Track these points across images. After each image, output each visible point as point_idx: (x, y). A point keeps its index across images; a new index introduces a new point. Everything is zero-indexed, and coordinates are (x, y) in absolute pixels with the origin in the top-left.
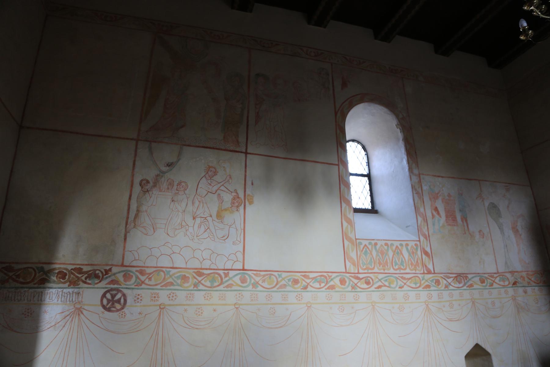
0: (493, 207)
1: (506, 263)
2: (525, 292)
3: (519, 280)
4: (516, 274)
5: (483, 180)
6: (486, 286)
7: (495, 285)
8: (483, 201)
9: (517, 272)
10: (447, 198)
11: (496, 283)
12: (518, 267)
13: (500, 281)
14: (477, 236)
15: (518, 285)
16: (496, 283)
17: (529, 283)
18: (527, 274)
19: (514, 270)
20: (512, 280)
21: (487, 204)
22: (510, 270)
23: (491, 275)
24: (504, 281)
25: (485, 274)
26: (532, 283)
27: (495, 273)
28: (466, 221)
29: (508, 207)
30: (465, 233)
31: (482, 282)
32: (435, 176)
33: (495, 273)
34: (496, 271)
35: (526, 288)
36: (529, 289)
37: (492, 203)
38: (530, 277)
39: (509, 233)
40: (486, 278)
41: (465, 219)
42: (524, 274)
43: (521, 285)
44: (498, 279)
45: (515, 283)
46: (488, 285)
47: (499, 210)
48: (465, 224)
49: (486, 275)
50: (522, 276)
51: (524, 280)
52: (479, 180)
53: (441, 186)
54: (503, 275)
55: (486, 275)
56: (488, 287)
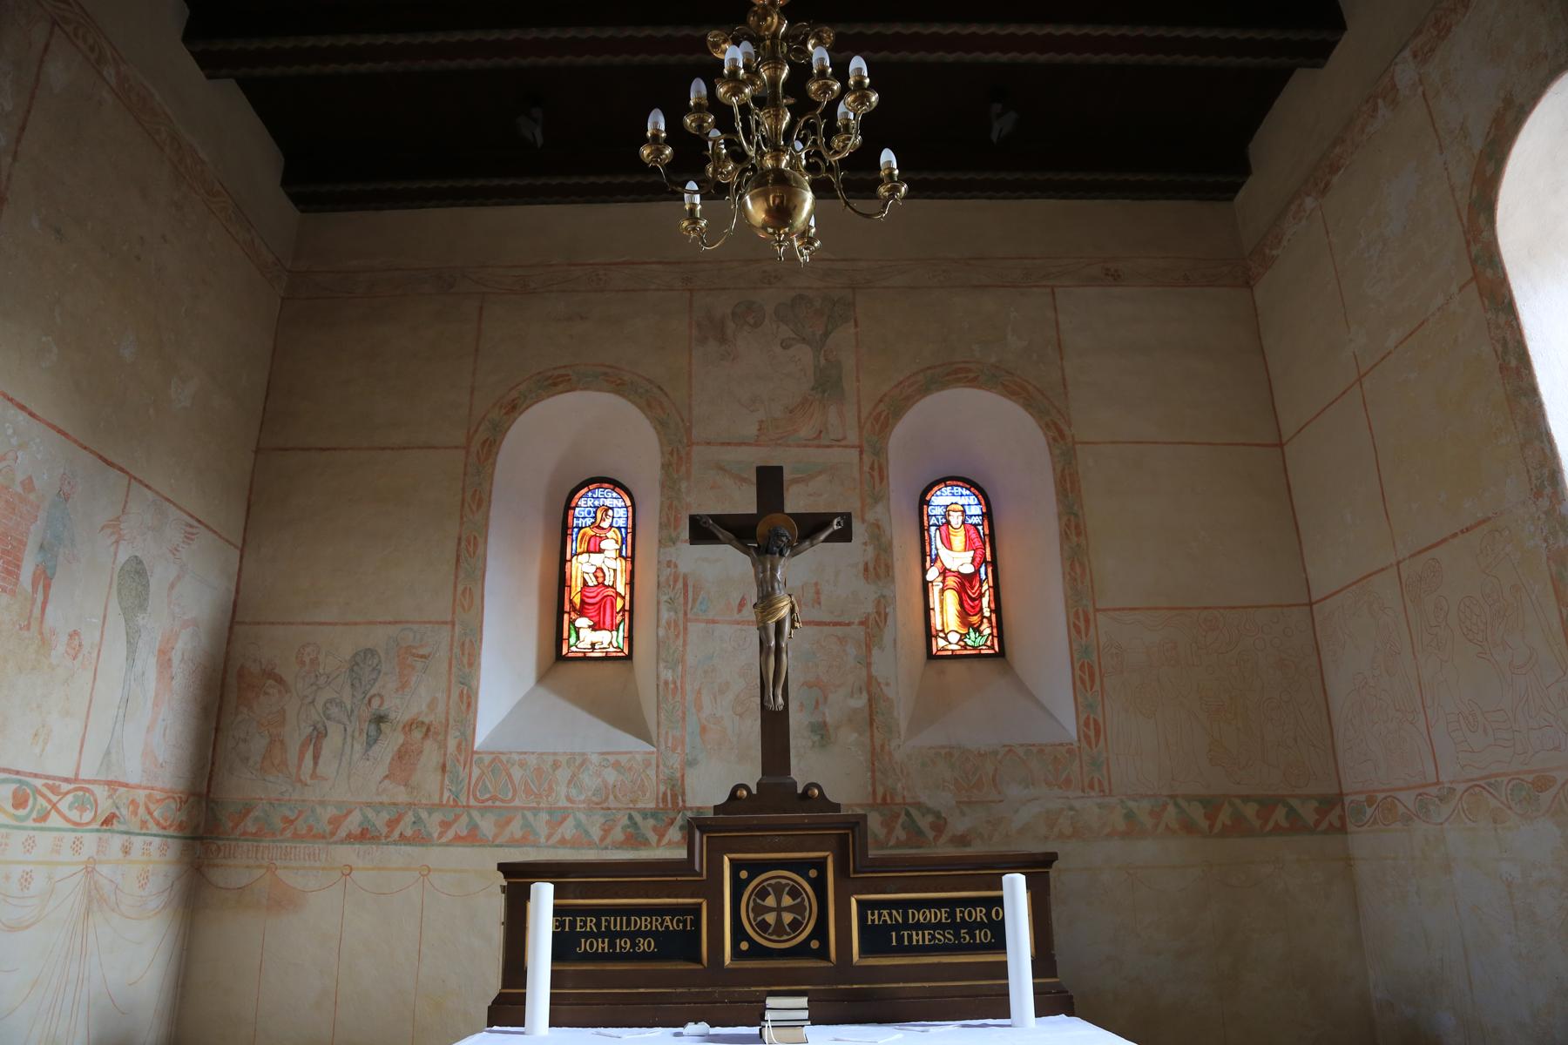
0: (137, 572)
1: (108, 753)
2: (126, 851)
3: (124, 811)
4: (123, 790)
5: (140, 482)
6: (27, 817)
7: (54, 820)
8: (117, 542)
9: (126, 785)
10: (19, 490)
11: (58, 811)
12: (133, 769)
13: (70, 808)
14: (61, 647)
15: (116, 826)
16: (58, 811)
17: (144, 823)
18: (149, 797)
19: (122, 780)
20: (105, 807)
21: (123, 557)
22: (110, 778)
23: (54, 785)
24: (82, 809)
25: (36, 776)
26: (151, 824)
27: (66, 780)
28: (47, 587)
29: (172, 586)
30: (28, 627)
31: (20, 801)
32: (11, 400)
33: (66, 780)
34: (71, 775)
35: (133, 838)
36: (138, 842)
37: (138, 561)
38: (152, 807)
39: (148, 662)
40: (37, 791)
41: (44, 579)
42: (141, 795)
43: (123, 828)
44: (70, 798)
45: (107, 821)
46: (34, 815)
47: (146, 586)
48: (40, 597)
49: (39, 783)
50: (133, 802)
51: (135, 813)
52: (131, 477)
53: (14, 441)
54: (87, 790)
55: (39, 783)
56: (30, 823)
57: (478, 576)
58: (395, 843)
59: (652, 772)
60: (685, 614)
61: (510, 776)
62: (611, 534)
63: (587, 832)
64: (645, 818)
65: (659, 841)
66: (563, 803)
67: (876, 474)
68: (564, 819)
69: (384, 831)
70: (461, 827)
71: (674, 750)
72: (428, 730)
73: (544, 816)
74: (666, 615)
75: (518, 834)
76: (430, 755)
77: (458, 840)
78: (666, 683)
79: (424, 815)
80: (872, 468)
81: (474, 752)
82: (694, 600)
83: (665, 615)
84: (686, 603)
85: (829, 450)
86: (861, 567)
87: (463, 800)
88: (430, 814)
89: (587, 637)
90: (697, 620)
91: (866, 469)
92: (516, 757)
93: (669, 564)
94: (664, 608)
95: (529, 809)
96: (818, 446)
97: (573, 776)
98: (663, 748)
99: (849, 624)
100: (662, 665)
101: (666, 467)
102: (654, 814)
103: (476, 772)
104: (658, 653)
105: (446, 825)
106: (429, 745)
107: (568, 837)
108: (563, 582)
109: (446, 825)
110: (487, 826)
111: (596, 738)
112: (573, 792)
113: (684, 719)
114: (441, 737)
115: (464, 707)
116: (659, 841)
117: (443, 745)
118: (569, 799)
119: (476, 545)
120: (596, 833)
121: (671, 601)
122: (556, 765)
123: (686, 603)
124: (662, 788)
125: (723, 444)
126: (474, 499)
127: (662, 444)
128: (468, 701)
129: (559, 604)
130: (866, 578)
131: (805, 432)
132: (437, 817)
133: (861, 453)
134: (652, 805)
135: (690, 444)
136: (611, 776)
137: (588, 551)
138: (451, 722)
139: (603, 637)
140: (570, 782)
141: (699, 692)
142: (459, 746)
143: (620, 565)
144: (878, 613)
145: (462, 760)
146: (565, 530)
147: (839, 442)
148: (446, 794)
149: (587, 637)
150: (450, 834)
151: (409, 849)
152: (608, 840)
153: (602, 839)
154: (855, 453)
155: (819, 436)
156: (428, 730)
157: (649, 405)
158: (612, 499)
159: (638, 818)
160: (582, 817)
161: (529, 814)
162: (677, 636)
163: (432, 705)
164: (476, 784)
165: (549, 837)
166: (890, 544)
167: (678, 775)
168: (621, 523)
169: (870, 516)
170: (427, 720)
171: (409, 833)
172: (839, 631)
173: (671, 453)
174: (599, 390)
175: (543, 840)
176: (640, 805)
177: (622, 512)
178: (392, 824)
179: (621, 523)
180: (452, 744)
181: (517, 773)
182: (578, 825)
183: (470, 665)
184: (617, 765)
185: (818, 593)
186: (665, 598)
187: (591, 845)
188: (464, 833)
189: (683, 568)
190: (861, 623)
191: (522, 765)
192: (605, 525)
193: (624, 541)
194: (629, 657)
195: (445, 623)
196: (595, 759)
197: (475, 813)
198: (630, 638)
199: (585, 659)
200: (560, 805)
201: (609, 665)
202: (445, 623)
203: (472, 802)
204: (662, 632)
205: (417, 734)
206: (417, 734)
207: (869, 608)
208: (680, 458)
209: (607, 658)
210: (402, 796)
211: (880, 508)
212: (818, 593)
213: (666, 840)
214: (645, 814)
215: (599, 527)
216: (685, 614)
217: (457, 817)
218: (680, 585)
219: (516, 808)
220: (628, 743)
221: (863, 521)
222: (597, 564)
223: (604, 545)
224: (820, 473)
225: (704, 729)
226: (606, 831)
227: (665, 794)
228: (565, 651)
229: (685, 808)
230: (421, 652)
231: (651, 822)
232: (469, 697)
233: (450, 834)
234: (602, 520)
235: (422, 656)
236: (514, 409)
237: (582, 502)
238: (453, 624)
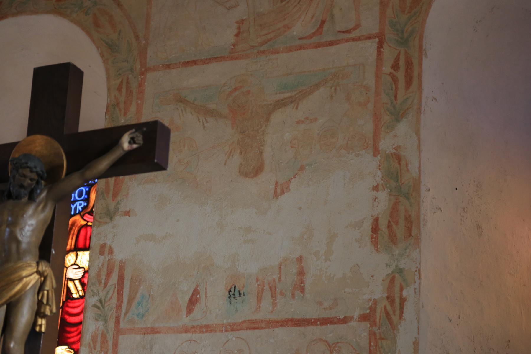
60: (117, 322)
67: (401, 75)
80: (395, 66)
82: (131, 300)
84: (119, 306)
85: (332, 49)
86: (368, 226)
90: (131, 331)
91: (387, 68)
96: (318, 46)
99: (345, 320)
123: (119, 306)
125: (187, 64)
127: (108, 79)
130: (375, 242)
131: (301, 27)
133: (380, 46)
135: (145, 70)
144: (390, 299)
147: (348, 35)
154: (371, 46)
155: (319, 31)
157: (97, 24)
166: (417, 184)
169: (386, 144)
172: (330, 332)
173: (119, 89)
174: (35, 12)
185: (301, 273)
189: (119, 256)
190: (364, 318)
207: (377, 291)
208: (130, 92)
211: (403, 128)
212: (301, 273)
216: (117, 322)
218: (114, 279)
221: (376, 152)
224: (317, 86)
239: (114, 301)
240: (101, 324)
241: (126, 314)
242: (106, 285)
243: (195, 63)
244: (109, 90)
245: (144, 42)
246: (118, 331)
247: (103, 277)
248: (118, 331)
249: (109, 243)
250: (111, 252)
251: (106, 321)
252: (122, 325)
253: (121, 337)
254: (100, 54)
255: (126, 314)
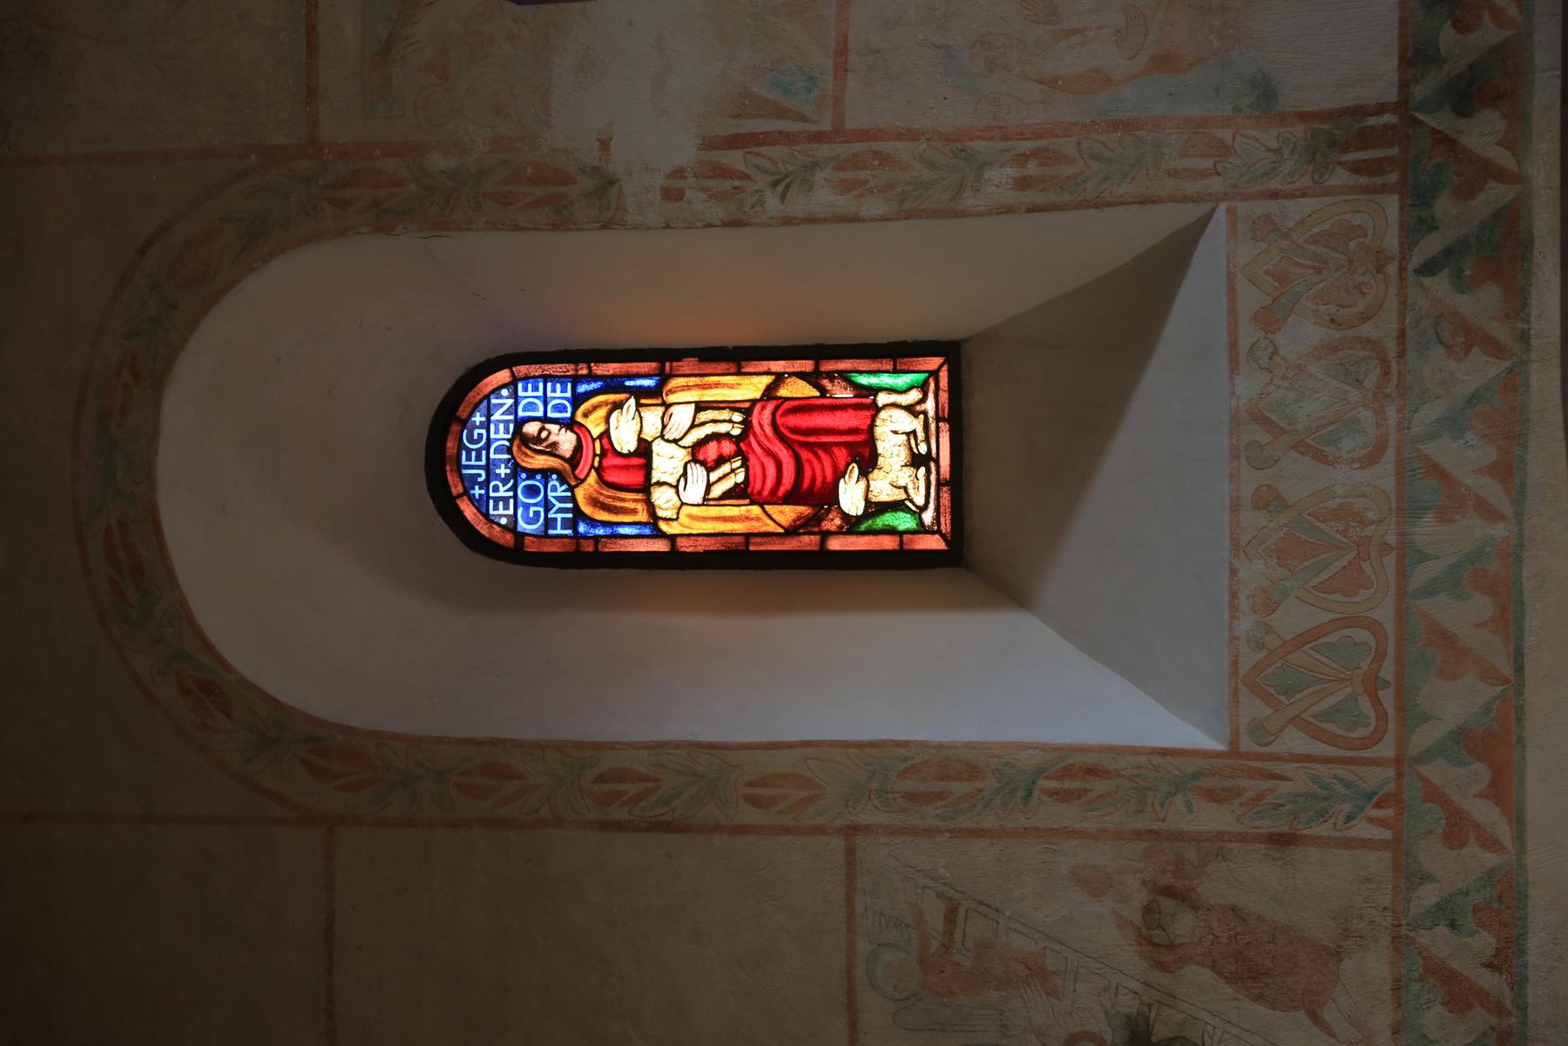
57: (709, 763)
58: (1518, 984)
59: (1296, 209)
60: (818, 137)
61: (1302, 640)
62: (595, 426)
63: (1473, 399)
64: (1430, 225)
65: (1504, 177)
66: (1384, 475)
68: (1435, 470)
69: (1480, 1018)
70: (1464, 782)
71: (1223, 150)
72: (1168, 892)
73: (1426, 530)
74: (824, 198)
75: (1483, 606)
76: (1247, 883)
77: (1502, 789)
78: (1023, 184)
79: (1428, 896)
81: (1234, 751)
82: (781, 113)
83: (824, 198)
84: (788, 138)
87: (1379, 778)
88: (1426, 878)
89: (894, 475)
92: (1246, 623)
93: (672, 195)
94: (799, 204)
95: (1402, 574)
97: (1301, 447)
98: (1216, 185)
100: (969, 201)
101: (384, 220)
102: (1418, 199)
103: (1294, 741)
104: (935, 214)
105: (1458, 829)
106: (1215, 888)
107: (1488, 454)
108: (732, 558)
109: (1458, 829)
110: (1455, 703)
111: (1182, 402)
112: (1350, 445)
113: (1129, 126)
114: (1191, 855)
115: (1098, 786)
116: (1504, 177)
117: (1216, 845)
118: (1373, 457)
119: (620, 776)
120: (1480, 370)
121: (782, 183)
122: (1270, 501)
123: (788, 138)
124: (1340, 177)
125: (312, 48)
126: (484, 789)
128: (1079, 773)
129: (800, 564)
132: (1433, 855)
134: (1392, 204)
136: (1304, 333)
137: (645, 487)
138: (1142, 823)
139: (893, 432)
140: (1321, 458)
141: (1051, 83)
142: (1213, 796)
143: (684, 394)
145: (1255, 786)
146: (585, 560)
148: (1362, 829)
149: (894, 475)
150: (1486, 814)
151: (1534, 942)
152: (1500, 332)
153: (1495, 349)
156: (1168, 892)
158: (493, 427)
159: (1432, 245)
160: (1427, 415)
161: (1420, 576)
162: (885, 159)
163: (1092, 883)
164: (1333, 740)
165: (1489, 513)
167: (1299, 131)
168: (560, 394)
170: (1140, 897)
171: (1484, 942)
175: (1499, 531)
176: (1392, 242)
177: (527, 393)
178: (1459, 995)
179: (560, 394)
180: (1212, 818)
181: (1293, 618)
182: (1452, 424)
183: (972, 771)
184: (1269, 319)
186: (772, 201)
187: (1514, 383)
188: (1481, 772)
189: (687, 152)
191: (1268, 603)
192: (566, 441)
193: (613, 384)
194: (952, 351)
195: (850, 852)
196: (1249, 385)
197: (1422, 738)
198: (896, 354)
199: (956, 485)
200: (1389, 483)
201: (980, 404)
202: (850, 852)
203: (1386, 749)
204: (874, 206)
205: (1184, 925)
206: (1184, 925)
209: (955, 417)
210: (1371, 967)
213: (1504, 159)
214: (1417, 226)
215: (575, 459)
216: (818, 137)
217: (1433, 794)
218: (733, 159)
219: (1401, 615)
220: (1198, 298)
222: (679, 457)
223: (625, 440)
225: (1164, 63)
226: (1470, 338)
227: (1356, 168)
228: (934, 543)
229: (1402, 105)
230: (936, 921)
231: (1444, 205)
232: (1067, 772)
233: (1486, 814)
234: (552, 450)
235: (951, 916)
236: (212, 687)
237: (502, 514)
238: (853, 831)
239: (778, 151)
240: (819, 177)
241: (804, 119)
242: (745, 176)
243: (311, 29)
244: (342, 232)
245: (253, 157)
246: (838, 133)
247: (728, 184)
248: (838, 133)
249: (660, 181)
250: (678, 173)
251: (816, 165)
252: (825, 126)
253: (849, 126)
254: (265, 262)
255: (804, 119)
